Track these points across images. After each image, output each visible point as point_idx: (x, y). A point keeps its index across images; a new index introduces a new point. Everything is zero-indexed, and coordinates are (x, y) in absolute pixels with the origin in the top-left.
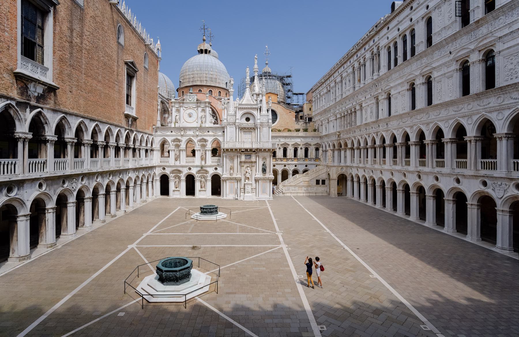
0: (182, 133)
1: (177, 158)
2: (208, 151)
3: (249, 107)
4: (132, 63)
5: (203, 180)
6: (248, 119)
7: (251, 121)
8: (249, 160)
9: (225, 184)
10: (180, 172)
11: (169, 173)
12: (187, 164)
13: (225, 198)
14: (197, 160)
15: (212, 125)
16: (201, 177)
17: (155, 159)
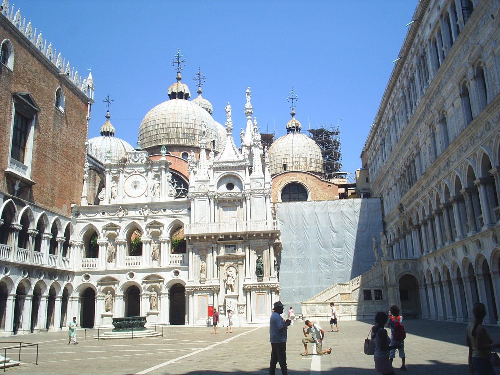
0: (121, 214)
1: (111, 257)
2: (164, 242)
3: (231, 165)
4: (27, 97)
5: (154, 294)
6: (230, 186)
7: (236, 189)
8: (233, 254)
9: (191, 299)
10: (114, 281)
11: (95, 284)
12: (128, 268)
13: (191, 324)
14: (145, 260)
15: (172, 199)
16: (150, 289)
17: (76, 259)
